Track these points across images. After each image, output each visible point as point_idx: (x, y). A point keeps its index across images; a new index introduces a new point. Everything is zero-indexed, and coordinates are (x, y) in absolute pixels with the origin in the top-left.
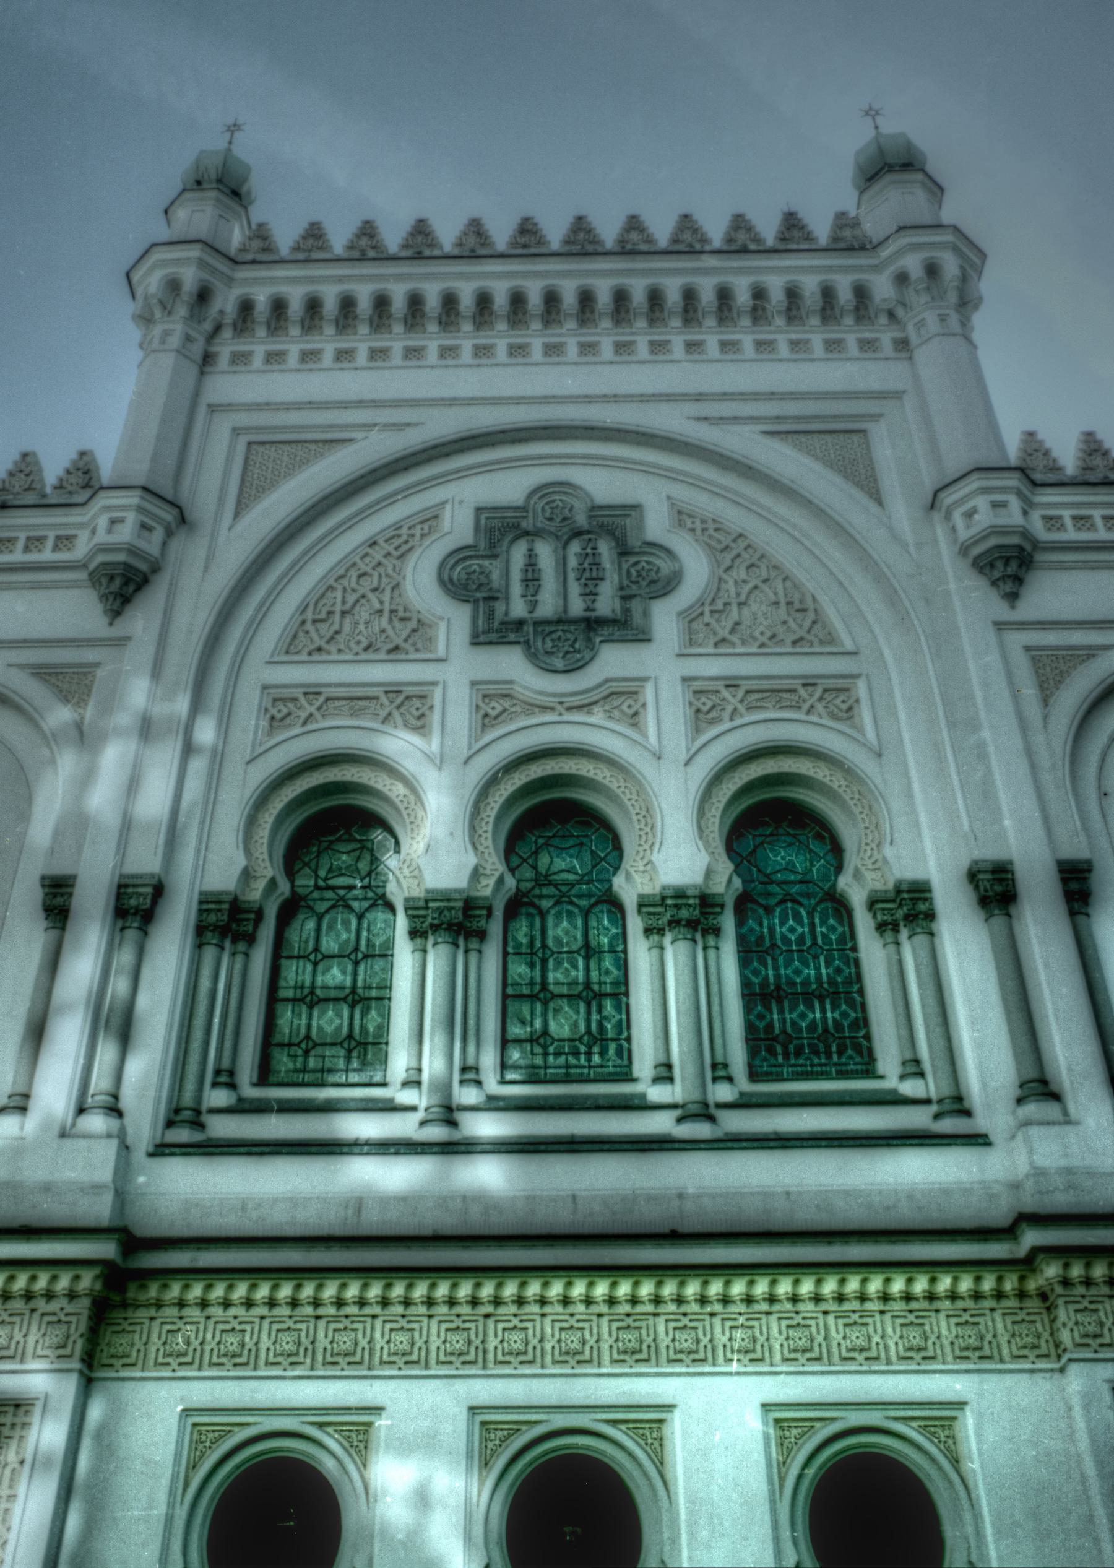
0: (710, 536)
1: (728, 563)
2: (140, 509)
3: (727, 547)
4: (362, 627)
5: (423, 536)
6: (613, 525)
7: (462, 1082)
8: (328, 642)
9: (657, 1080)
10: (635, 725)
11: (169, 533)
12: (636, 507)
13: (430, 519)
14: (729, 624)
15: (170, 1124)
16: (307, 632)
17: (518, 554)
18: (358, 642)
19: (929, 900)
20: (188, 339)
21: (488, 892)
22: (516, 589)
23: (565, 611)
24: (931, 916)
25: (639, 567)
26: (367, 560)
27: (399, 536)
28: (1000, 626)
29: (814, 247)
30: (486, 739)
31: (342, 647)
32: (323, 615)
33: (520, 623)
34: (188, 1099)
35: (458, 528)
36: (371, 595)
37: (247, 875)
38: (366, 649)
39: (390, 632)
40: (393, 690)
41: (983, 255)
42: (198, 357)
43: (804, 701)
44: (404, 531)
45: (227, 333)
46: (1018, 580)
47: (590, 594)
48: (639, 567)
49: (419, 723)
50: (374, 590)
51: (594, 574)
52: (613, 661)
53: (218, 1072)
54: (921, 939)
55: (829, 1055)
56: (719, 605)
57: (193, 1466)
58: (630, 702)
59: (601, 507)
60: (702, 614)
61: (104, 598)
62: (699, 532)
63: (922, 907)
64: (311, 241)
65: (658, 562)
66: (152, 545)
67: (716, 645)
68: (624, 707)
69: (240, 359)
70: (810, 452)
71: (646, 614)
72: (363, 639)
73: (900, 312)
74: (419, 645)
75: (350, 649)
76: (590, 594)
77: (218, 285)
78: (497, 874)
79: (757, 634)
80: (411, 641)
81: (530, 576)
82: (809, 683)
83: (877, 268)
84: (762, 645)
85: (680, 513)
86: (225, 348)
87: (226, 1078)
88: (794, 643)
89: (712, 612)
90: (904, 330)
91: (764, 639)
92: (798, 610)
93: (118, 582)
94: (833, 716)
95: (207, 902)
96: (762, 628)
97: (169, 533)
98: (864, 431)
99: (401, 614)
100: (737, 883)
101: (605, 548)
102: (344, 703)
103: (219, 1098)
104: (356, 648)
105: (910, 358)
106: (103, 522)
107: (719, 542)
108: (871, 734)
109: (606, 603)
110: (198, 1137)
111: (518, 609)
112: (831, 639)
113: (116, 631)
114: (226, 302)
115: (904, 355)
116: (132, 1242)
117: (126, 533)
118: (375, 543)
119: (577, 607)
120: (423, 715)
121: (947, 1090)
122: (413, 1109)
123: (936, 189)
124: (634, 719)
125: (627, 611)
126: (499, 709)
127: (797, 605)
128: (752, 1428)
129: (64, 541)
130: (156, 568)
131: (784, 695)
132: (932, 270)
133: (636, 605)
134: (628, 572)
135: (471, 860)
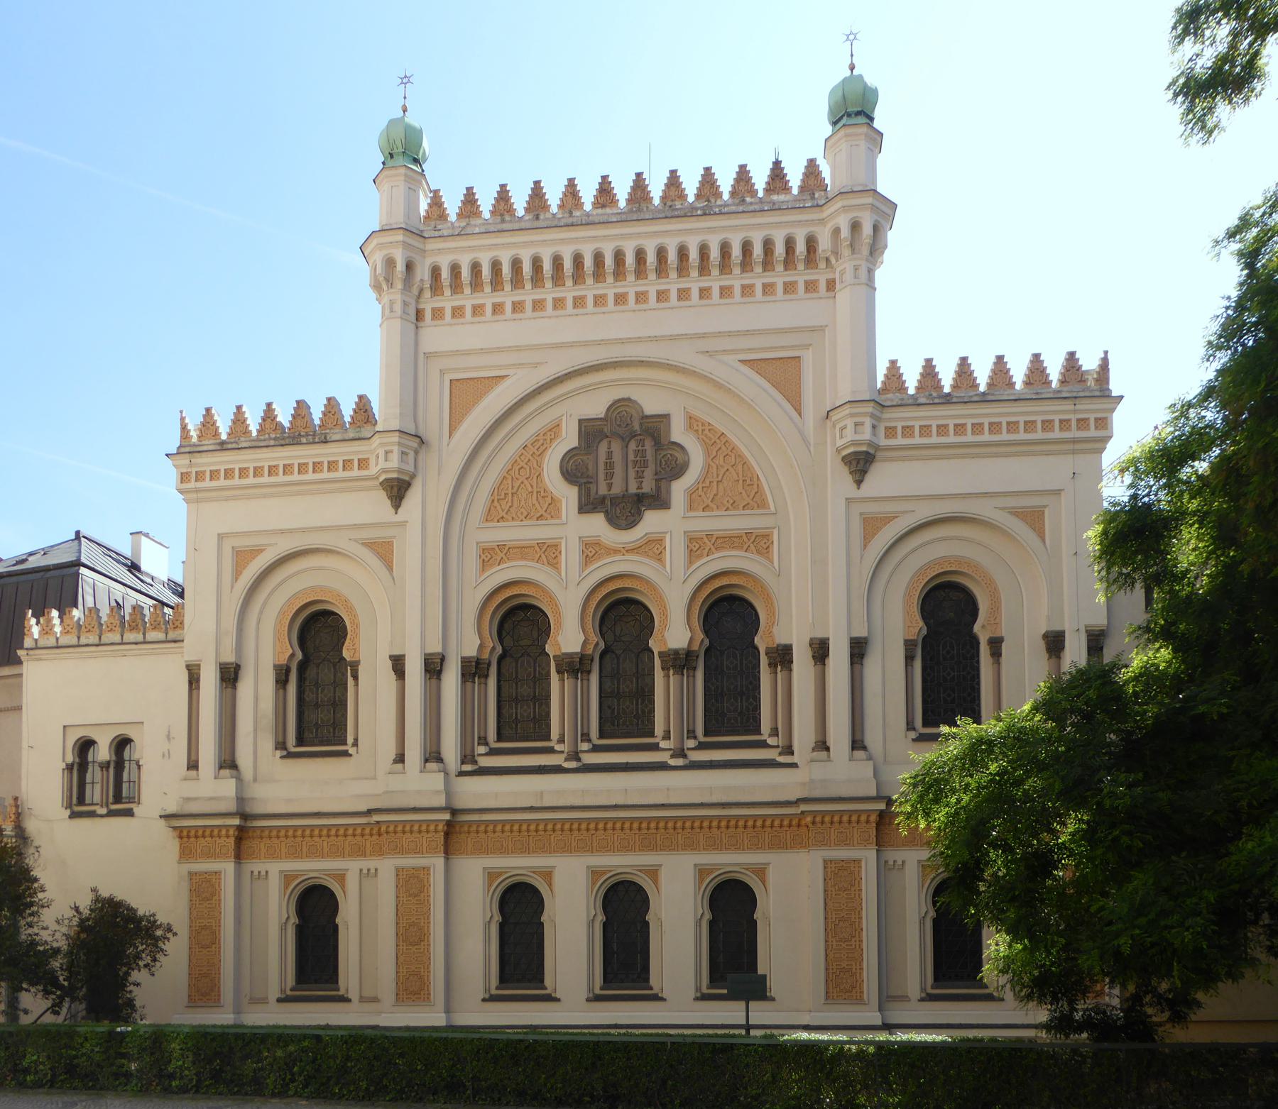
2: (399, 444)
6: (652, 430)
11: (416, 452)
12: (666, 417)
13: (554, 430)
15: (463, 763)
17: (603, 448)
20: (405, 304)
21: (590, 652)
22: (601, 476)
30: (586, 572)
33: (604, 498)
34: (468, 752)
35: (570, 439)
37: (481, 647)
42: (413, 318)
45: (427, 294)
47: (640, 477)
52: (652, 521)
53: (479, 738)
54: (785, 672)
57: (490, 885)
59: (647, 417)
61: (390, 497)
65: (677, 455)
66: (411, 468)
69: (438, 314)
71: (669, 492)
76: (640, 477)
77: (417, 259)
86: (428, 304)
87: (483, 741)
93: (396, 489)
94: (759, 553)
95: (465, 662)
97: (416, 452)
100: (707, 642)
101: (648, 445)
103: (482, 749)
106: (381, 452)
108: (776, 564)
109: (648, 487)
110: (475, 767)
111: (603, 490)
112: (763, 504)
116: (454, 812)
117: (394, 462)
119: (633, 489)
124: (659, 558)
125: (658, 488)
128: (689, 875)
129: (363, 463)
130: (413, 476)
133: (663, 484)
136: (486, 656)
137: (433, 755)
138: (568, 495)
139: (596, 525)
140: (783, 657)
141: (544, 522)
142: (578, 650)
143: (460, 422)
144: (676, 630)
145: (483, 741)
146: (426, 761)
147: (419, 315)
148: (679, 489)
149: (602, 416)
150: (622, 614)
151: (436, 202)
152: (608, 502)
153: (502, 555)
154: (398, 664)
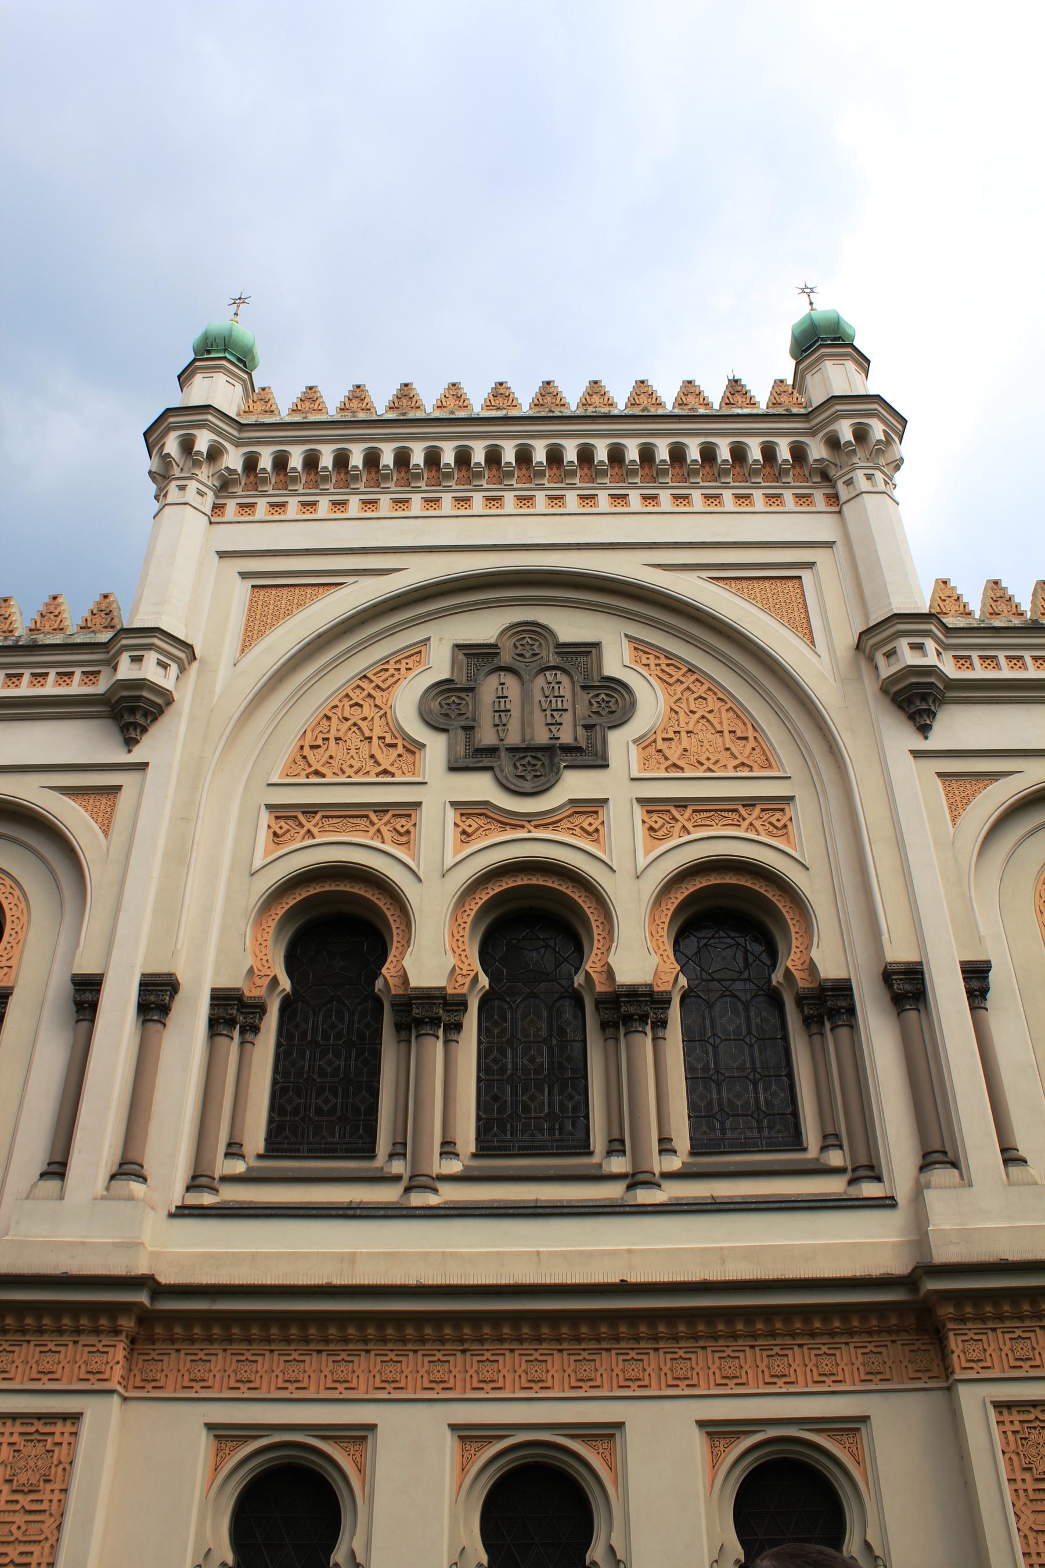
0: (663, 671)
1: (679, 695)
3: (678, 680)
4: (353, 752)
5: (407, 669)
7: (441, 1154)
8: (323, 766)
9: (610, 1153)
10: (596, 841)
12: (597, 645)
14: (680, 751)
15: (189, 1189)
16: (305, 757)
17: (489, 687)
18: (351, 766)
19: (851, 996)
21: (464, 990)
23: (532, 739)
24: (851, 1011)
25: (599, 699)
26: (358, 691)
27: (387, 670)
28: (917, 754)
29: (755, 411)
31: (335, 771)
32: (320, 742)
33: (492, 751)
35: (439, 665)
36: (363, 725)
38: (356, 773)
39: (379, 756)
40: (381, 809)
41: (904, 422)
43: (744, 819)
44: (391, 666)
46: (932, 714)
48: (599, 699)
49: (404, 839)
50: (364, 719)
51: (560, 706)
52: (575, 784)
54: (844, 1032)
55: (760, 1129)
56: (671, 735)
58: (590, 820)
60: (655, 741)
62: (653, 667)
63: (844, 1004)
64: (307, 404)
67: (666, 769)
68: (585, 825)
70: (752, 599)
72: (354, 763)
73: (832, 472)
74: (405, 769)
75: (343, 772)
78: (473, 974)
79: (703, 759)
80: (396, 765)
81: (502, 708)
82: (749, 803)
83: (812, 433)
84: (710, 770)
85: (635, 649)
87: (234, 1150)
88: (735, 767)
89: (664, 739)
90: (834, 487)
91: (708, 764)
92: (739, 738)
94: (770, 834)
96: (707, 754)
97: (182, 669)
98: (800, 578)
99: (388, 741)
102: (338, 820)
104: (349, 771)
105: (840, 512)
107: (672, 676)
113: (137, 755)
114: (233, 459)
115: (836, 509)
118: (365, 677)
120: (408, 832)
121: (863, 1161)
122: (397, 1178)
123: (863, 362)
126: (475, 826)
127: (739, 734)
131: (726, 814)
132: (861, 434)
134: (591, 704)
135: (451, 960)
136: (256, 993)
137: (128, 1169)
138: (436, 748)
139: (480, 787)
140: (831, 1005)
141: (389, 779)
142: (443, 984)
143: (261, 634)
144: (636, 952)
145: (234, 1150)
146: (113, 1177)
147: (218, 508)
148: (620, 743)
149: (492, 641)
150: (534, 920)
151: (264, 397)
152: (503, 754)
153: (308, 826)
154: (86, 994)
